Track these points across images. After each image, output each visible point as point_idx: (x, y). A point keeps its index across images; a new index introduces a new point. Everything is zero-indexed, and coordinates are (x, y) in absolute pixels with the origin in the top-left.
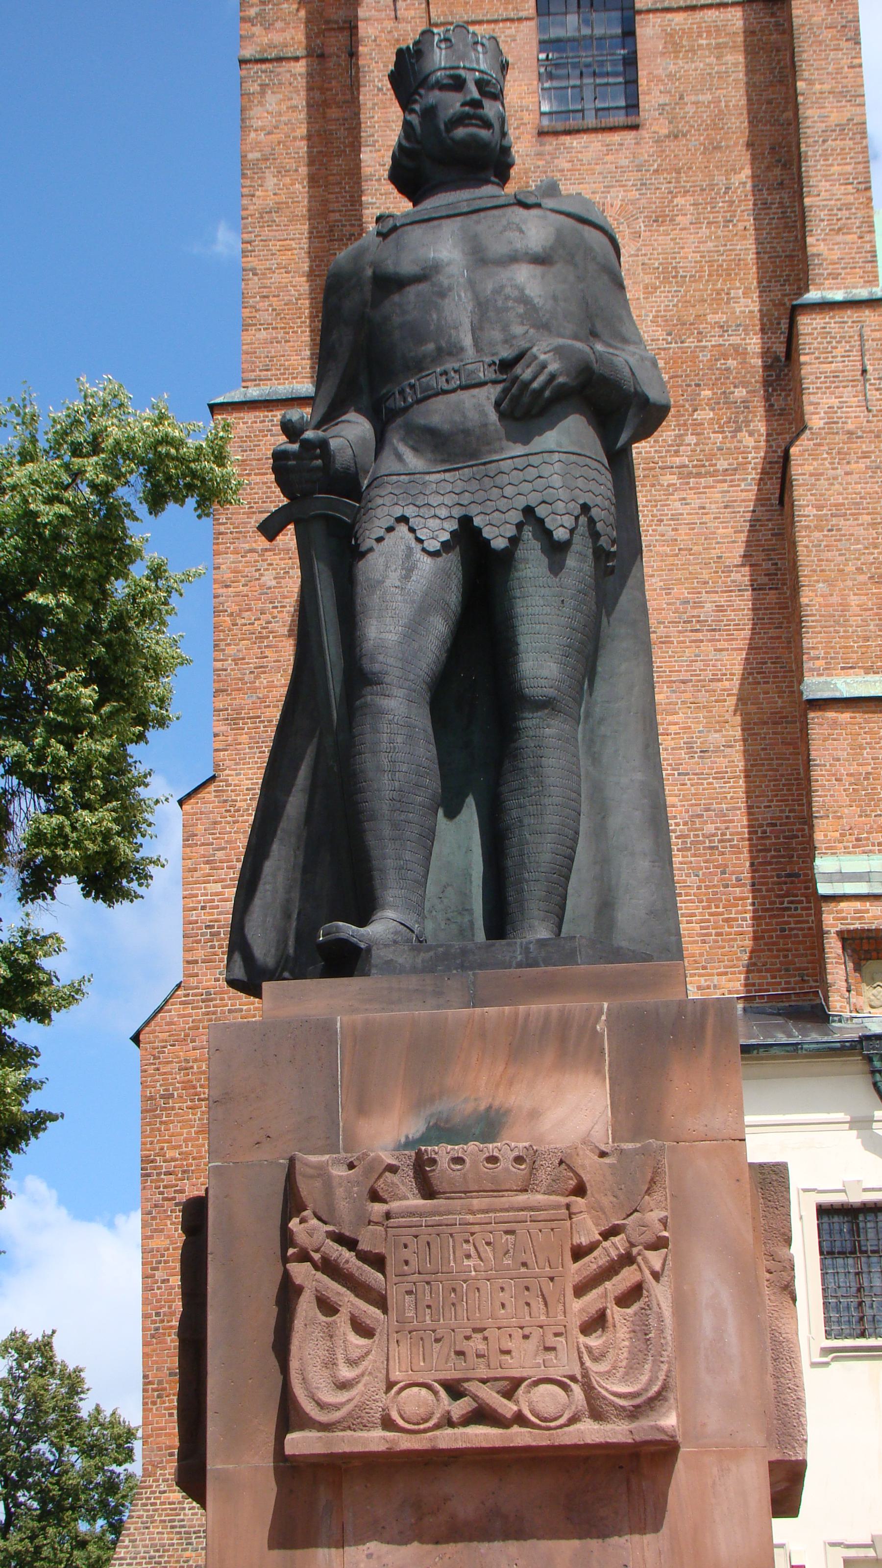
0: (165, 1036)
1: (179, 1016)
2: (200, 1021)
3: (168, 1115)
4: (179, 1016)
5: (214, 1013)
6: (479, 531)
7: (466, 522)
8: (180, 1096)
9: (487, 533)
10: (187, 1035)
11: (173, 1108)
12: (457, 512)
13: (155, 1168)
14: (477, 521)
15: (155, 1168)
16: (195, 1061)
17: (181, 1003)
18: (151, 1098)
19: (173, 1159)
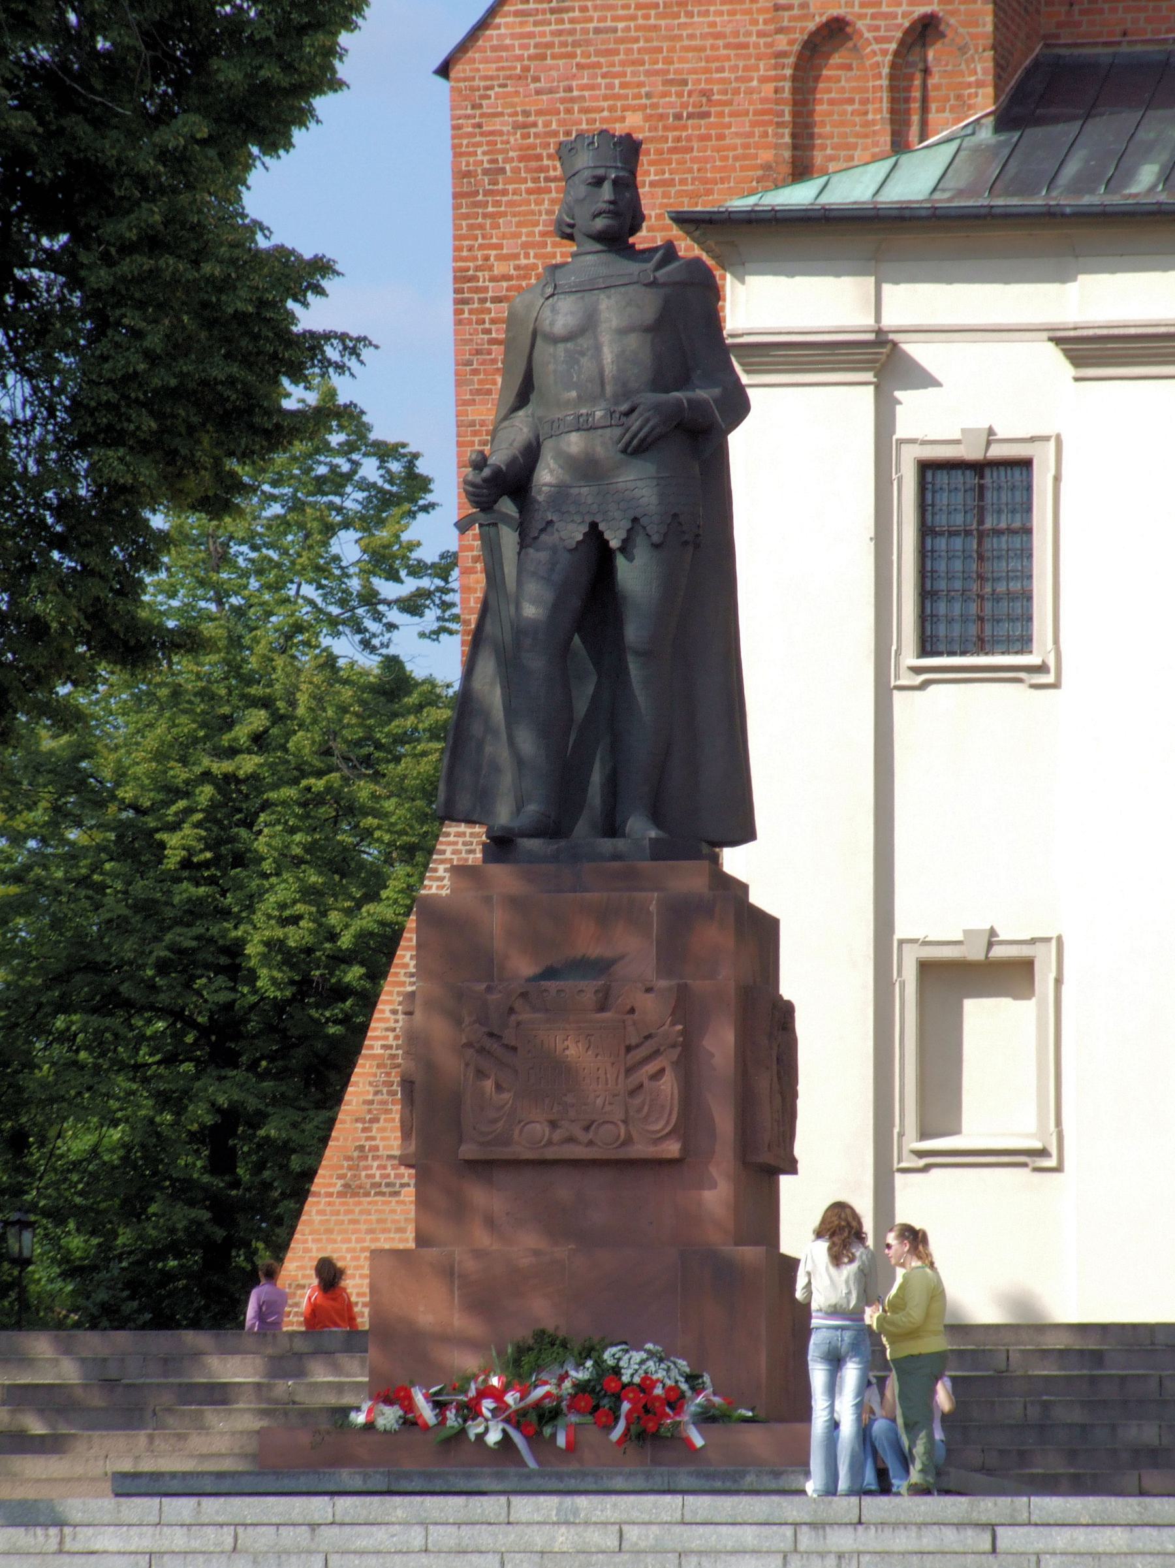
0: (490, 69)
1: (513, 36)
2: (550, 45)
3: (497, 204)
4: (513, 36)
5: (572, 32)
6: (601, 534)
7: (594, 526)
8: (516, 170)
9: (607, 536)
10: (526, 69)
11: (504, 192)
12: (589, 519)
13: (477, 290)
14: (601, 527)
15: (477, 290)
16: (539, 113)
17: (517, 13)
18: (468, 174)
19: (506, 278)
